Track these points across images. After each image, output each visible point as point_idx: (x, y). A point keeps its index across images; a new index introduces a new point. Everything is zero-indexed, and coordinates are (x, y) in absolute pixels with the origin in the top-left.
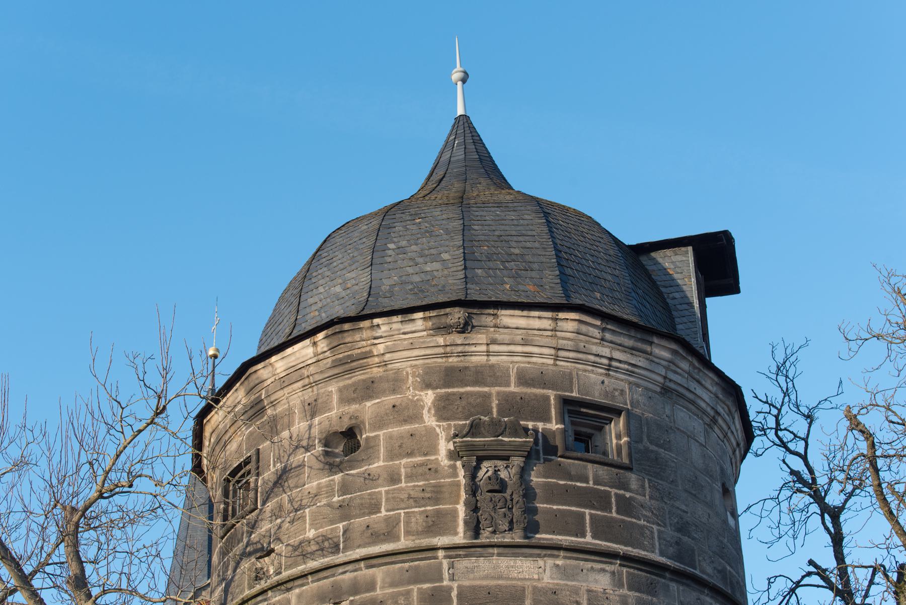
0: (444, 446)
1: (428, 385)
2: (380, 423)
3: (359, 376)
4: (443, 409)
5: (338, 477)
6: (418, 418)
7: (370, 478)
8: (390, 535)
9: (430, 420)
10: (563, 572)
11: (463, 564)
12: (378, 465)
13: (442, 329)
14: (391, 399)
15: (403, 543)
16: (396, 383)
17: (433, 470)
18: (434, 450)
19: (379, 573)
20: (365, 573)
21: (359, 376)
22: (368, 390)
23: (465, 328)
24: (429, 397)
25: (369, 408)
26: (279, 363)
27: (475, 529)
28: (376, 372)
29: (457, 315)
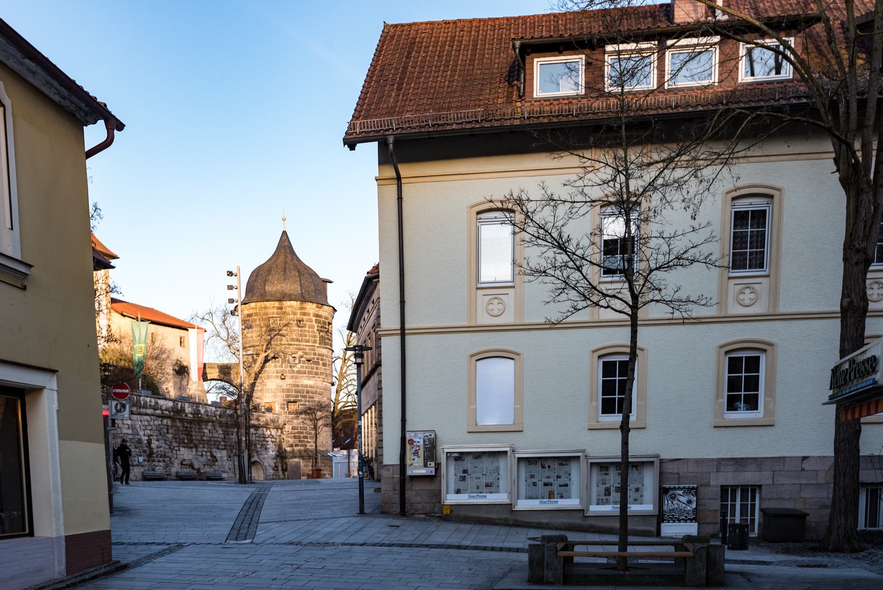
0: (316, 328)
1: (314, 316)
2: (307, 321)
3: (303, 311)
4: (316, 321)
5: (300, 329)
6: (312, 322)
7: (305, 331)
8: (309, 342)
9: (314, 323)
10: (328, 352)
11: (318, 349)
12: (307, 329)
13: (317, 307)
14: (308, 317)
15: (310, 344)
16: (309, 314)
17: (314, 332)
18: (314, 328)
19: (307, 348)
20: (305, 347)
21: (303, 311)
22: (305, 314)
23: (320, 308)
24: (314, 319)
25: (305, 318)
26: (288, 303)
27: (320, 343)
28: (306, 311)
29: (320, 306)
